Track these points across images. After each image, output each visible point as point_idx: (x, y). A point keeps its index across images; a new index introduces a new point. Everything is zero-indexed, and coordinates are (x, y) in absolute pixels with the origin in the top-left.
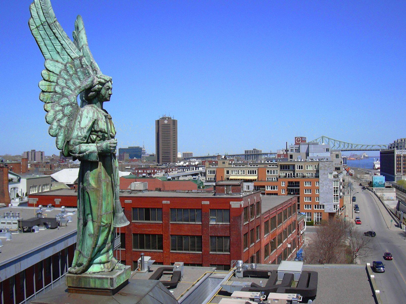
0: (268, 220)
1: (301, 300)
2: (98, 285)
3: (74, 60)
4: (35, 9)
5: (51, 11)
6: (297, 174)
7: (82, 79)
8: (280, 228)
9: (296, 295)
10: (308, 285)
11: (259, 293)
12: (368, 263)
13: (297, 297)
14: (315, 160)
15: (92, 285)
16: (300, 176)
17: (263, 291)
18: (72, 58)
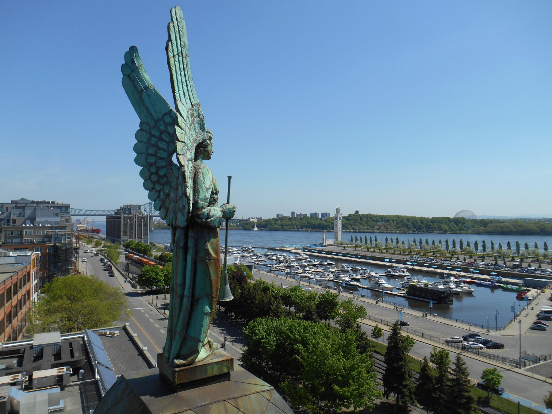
0: (3, 293)
1: (72, 373)
2: (215, 371)
3: (193, 107)
4: (173, 31)
5: (186, 41)
6: (25, 240)
7: (197, 131)
8: (15, 300)
9: (65, 368)
10: (72, 356)
11: (20, 375)
12: (127, 322)
13: (67, 370)
14: (46, 225)
15: (210, 374)
16: (28, 242)
17: (24, 371)
18: (193, 104)
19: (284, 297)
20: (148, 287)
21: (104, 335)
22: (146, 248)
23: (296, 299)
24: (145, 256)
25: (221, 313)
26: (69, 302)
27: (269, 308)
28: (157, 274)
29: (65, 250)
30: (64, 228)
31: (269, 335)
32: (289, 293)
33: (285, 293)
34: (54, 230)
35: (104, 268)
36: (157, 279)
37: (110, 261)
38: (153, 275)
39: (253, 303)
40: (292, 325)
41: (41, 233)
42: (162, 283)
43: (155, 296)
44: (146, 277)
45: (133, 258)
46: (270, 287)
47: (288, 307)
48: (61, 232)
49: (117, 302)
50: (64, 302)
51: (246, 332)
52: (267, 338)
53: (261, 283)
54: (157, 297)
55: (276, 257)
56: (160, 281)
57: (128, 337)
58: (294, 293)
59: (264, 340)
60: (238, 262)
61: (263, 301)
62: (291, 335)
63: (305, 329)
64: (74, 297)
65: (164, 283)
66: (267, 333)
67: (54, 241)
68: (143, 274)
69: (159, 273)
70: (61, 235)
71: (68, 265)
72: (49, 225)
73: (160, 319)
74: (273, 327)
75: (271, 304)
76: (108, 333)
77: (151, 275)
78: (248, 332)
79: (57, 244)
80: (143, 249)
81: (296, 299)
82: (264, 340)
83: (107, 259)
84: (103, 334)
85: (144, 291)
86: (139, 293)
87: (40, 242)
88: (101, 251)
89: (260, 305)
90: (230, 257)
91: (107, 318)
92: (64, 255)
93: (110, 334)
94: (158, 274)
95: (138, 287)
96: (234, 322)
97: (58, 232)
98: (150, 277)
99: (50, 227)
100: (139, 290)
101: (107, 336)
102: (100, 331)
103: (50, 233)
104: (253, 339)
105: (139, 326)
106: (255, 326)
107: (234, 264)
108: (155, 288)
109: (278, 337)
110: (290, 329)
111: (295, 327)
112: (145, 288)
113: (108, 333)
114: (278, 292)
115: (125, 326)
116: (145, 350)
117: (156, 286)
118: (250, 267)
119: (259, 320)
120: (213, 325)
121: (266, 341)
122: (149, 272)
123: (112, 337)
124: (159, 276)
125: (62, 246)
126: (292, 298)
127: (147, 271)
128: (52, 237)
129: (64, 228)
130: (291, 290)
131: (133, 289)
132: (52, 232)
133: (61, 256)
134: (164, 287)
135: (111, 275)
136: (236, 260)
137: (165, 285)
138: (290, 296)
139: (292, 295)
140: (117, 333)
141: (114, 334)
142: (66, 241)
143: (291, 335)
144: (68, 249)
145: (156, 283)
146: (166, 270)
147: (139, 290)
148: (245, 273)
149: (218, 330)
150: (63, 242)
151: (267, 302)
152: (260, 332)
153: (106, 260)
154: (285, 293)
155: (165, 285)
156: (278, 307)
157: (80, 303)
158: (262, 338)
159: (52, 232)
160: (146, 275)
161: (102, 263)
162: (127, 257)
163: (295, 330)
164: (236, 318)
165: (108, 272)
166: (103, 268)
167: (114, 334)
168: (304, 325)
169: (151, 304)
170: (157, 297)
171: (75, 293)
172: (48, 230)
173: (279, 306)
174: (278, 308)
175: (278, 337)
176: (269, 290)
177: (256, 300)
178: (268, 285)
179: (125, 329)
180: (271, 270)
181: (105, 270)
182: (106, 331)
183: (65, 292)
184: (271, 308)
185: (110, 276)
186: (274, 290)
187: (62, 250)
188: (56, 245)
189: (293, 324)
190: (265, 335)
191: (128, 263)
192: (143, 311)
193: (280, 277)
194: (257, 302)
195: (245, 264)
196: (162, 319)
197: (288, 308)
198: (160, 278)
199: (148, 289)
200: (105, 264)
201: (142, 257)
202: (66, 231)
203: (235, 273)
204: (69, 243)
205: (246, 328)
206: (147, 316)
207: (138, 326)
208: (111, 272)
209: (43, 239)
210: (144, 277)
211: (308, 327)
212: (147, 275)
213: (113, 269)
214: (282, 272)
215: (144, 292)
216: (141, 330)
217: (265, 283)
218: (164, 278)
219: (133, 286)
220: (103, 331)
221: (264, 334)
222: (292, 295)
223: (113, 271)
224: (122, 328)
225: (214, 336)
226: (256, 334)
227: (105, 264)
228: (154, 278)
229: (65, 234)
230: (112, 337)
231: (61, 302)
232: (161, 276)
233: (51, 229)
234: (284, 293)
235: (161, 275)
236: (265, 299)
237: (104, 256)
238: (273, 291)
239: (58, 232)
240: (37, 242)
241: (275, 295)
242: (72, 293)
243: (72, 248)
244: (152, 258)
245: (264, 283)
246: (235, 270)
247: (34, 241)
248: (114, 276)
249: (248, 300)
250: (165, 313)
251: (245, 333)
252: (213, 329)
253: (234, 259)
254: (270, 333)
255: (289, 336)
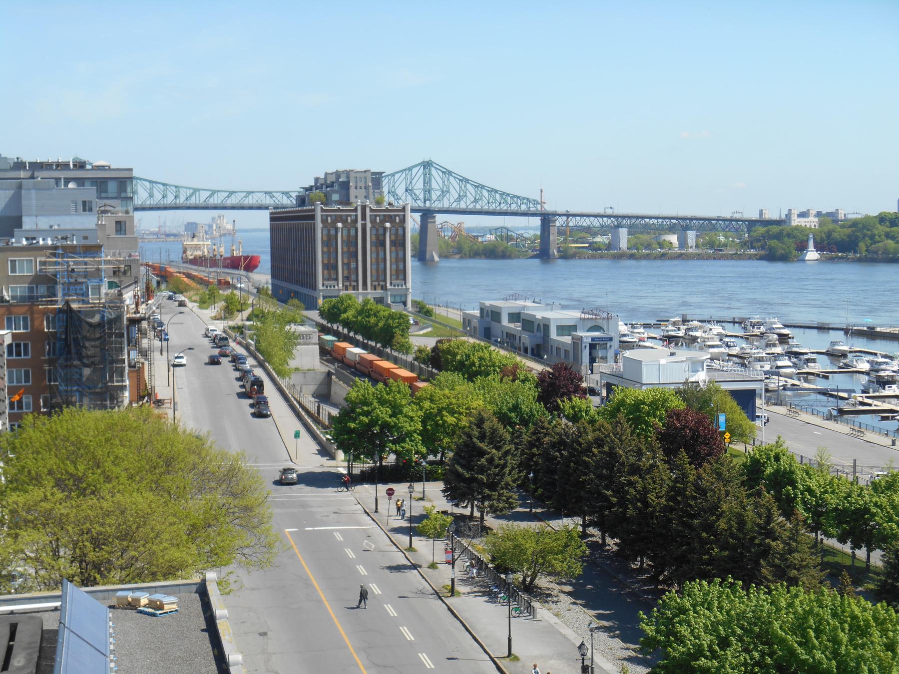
14: (41, 242)
19: (845, 510)
20: (370, 455)
21: (133, 606)
22: (390, 321)
23: (891, 520)
24: (388, 350)
25: (608, 557)
26: (60, 495)
27: (766, 552)
28: (396, 411)
29: (100, 325)
30: (93, 250)
31: (724, 643)
32: (867, 498)
33: (849, 495)
34: (63, 256)
35: (243, 386)
36: (399, 429)
37: (261, 365)
38: (383, 413)
39: (709, 527)
40: (810, 612)
41: (27, 268)
42: (415, 446)
43: (382, 488)
44: (361, 421)
45: (348, 355)
46: (799, 475)
47: (860, 548)
48: (86, 263)
49: (242, 502)
50: (46, 497)
51: (649, 630)
52: (714, 656)
53: (768, 458)
54: (390, 493)
55: (871, 363)
56: (409, 434)
57: (206, 618)
58: (883, 500)
59: (703, 661)
60: (701, 377)
61: (742, 523)
62: (800, 650)
63: (859, 630)
64: (79, 480)
65: (424, 442)
66: (718, 637)
67: (64, 295)
68: (353, 411)
69: (405, 410)
70: (86, 275)
71: (111, 377)
72: (50, 242)
73: (391, 568)
74: (741, 616)
75: (771, 534)
76: (144, 601)
77: (378, 419)
78: (658, 631)
79: (74, 306)
80: (381, 324)
81: (891, 520)
82: (703, 661)
83: (255, 358)
84: (129, 604)
85: (357, 468)
86: (340, 476)
87: (23, 299)
88: (240, 329)
89: (732, 536)
90: (673, 359)
91: (175, 554)
92: (97, 343)
93: (151, 604)
94: (401, 412)
95: (341, 455)
96: (647, 592)
97: (76, 263)
98: (373, 423)
99: (55, 248)
100: (340, 464)
101: (141, 612)
102: (120, 594)
103: (51, 269)
104: (667, 656)
105: (318, 588)
106: (683, 611)
107: (686, 383)
108: (391, 459)
109: (756, 655)
110: (800, 628)
111: (820, 621)
112: (356, 458)
113: (144, 601)
114: (826, 492)
115: (204, 582)
116: (236, 664)
117: (396, 452)
118: (746, 399)
119: (699, 588)
120: (569, 599)
121: (709, 664)
122: (371, 404)
123: (154, 615)
124: (402, 419)
125: (92, 314)
126: (874, 515)
127: (365, 402)
128: (56, 283)
129: (93, 250)
130: (875, 487)
131: (324, 461)
132: (56, 263)
133: (87, 344)
134: (424, 457)
135: (261, 412)
136: (695, 371)
137: (424, 450)
138: (867, 510)
139: (876, 505)
140: (170, 602)
141: (161, 607)
142: (103, 296)
143: (800, 650)
144: (111, 322)
145: (394, 442)
146: (432, 400)
147: (340, 464)
148: (722, 419)
149: (584, 616)
150: (92, 298)
151: (758, 525)
152: (692, 632)
153: (250, 362)
154: (849, 495)
155: (424, 450)
156: (789, 544)
157: (92, 501)
158: (698, 653)
159: (56, 263)
160: (360, 414)
161: (237, 369)
162: (326, 352)
163: (818, 632)
164: (654, 580)
165: (251, 401)
166: (237, 387)
167: (161, 607)
168: (854, 617)
169: (373, 513)
170: (390, 493)
171: (81, 468)
172: (43, 259)
173: (794, 544)
174: (791, 552)
175: (756, 655)
176: (793, 483)
177: (719, 516)
178: (791, 466)
179: (202, 591)
180: (841, 412)
181: (241, 395)
182: (137, 594)
183: (52, 462)
184: (769, 546)
185: (254, 415)
186: (813, 484)
187: (90, 325)
188: (71, 309)
189: (811, 609)
190: (710, 646)
191: (329, 374)
192: (339, 537)
193: (870, 436)
194: (722, 524)
195: (725, 387)
196: (399, 568)
197: (861, 553)
198: (407, 427)
199: (369, 464)
200: (244, 375)
201: (380, 354)
202: (99, 263)
203: (677, 415)
204: (111, 302)
205: (648, 612)
206: (351, 554)
207: (313, 587)
208: (258, 403)
209: (31, 289)
210: (354, 420)
211: (868, 626)
212: (367, 414)
213: (269, 390)
214: (884, 418)
215: (356, 471)
216: (320, 602)
217: (783, 459)
218: (424, 422)
219: (325, 452)
220: (130, 596)
221: (706, 640)
222: (876, 505)
223: (265, 398)
224: (194, 588)
225: (564, 636)
226: (680, 640)
227: (244, 375)
228: (385, 426)
229: (98, 270)
230: (154, 615)
231: (36, 493)
232: (411, 419)
233: (54, 255)
234: (845, 498)
235: (411, 414)
236: (750, 514)
237: (247, 348)
238: (810, 490)
239: (76, 263)
240: (13, 297)
241: (818, 505)
242: (71, 469)
243: (119, 318)
244: (410, 358)
245: (777, 458)
246: (677, 403)
247: (5, 293)
248: (266, 416)
249: (694, 517)
250: (410, 548)
251: (644, 631)
252: (567, 614)
253: (686, 366)
254: (727, 638)
255: (792, 652)
